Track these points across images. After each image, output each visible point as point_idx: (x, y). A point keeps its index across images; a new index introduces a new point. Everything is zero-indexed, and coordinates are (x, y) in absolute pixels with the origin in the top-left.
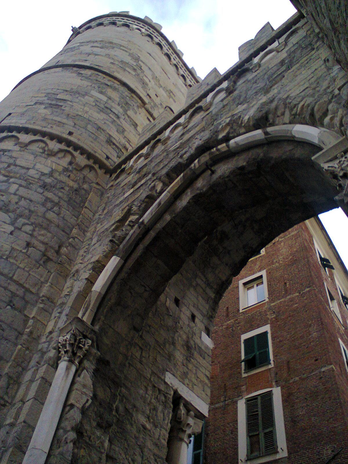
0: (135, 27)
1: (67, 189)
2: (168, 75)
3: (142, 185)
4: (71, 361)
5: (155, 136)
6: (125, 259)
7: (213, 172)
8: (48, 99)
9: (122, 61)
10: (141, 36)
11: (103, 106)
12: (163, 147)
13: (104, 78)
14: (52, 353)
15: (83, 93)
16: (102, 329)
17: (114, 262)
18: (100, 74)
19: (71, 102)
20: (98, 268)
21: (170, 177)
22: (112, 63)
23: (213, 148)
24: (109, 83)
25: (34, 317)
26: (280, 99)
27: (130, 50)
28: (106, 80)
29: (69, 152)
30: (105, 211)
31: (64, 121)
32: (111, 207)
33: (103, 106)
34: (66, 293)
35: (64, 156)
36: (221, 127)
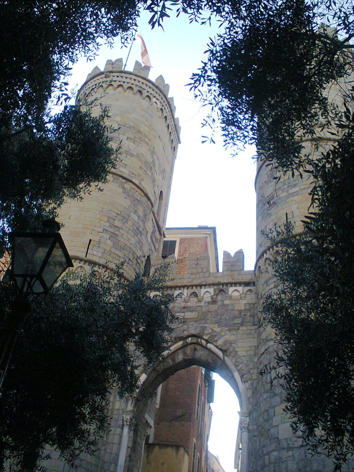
0: (154, 100)
4: (129, 429)
6: (148, 376)
7: (195, 349)
9: (146, 161)
11: (135, 229)
14: (121, 422)
15: (127, 217)
16: (137, 411)
18: (135, 187)
23: (200, 338)
24: (139, 197)
25: (112, 402)
26: (234, 349)
27: (150, 140)
28: (138, 195)
33: (135, 229)
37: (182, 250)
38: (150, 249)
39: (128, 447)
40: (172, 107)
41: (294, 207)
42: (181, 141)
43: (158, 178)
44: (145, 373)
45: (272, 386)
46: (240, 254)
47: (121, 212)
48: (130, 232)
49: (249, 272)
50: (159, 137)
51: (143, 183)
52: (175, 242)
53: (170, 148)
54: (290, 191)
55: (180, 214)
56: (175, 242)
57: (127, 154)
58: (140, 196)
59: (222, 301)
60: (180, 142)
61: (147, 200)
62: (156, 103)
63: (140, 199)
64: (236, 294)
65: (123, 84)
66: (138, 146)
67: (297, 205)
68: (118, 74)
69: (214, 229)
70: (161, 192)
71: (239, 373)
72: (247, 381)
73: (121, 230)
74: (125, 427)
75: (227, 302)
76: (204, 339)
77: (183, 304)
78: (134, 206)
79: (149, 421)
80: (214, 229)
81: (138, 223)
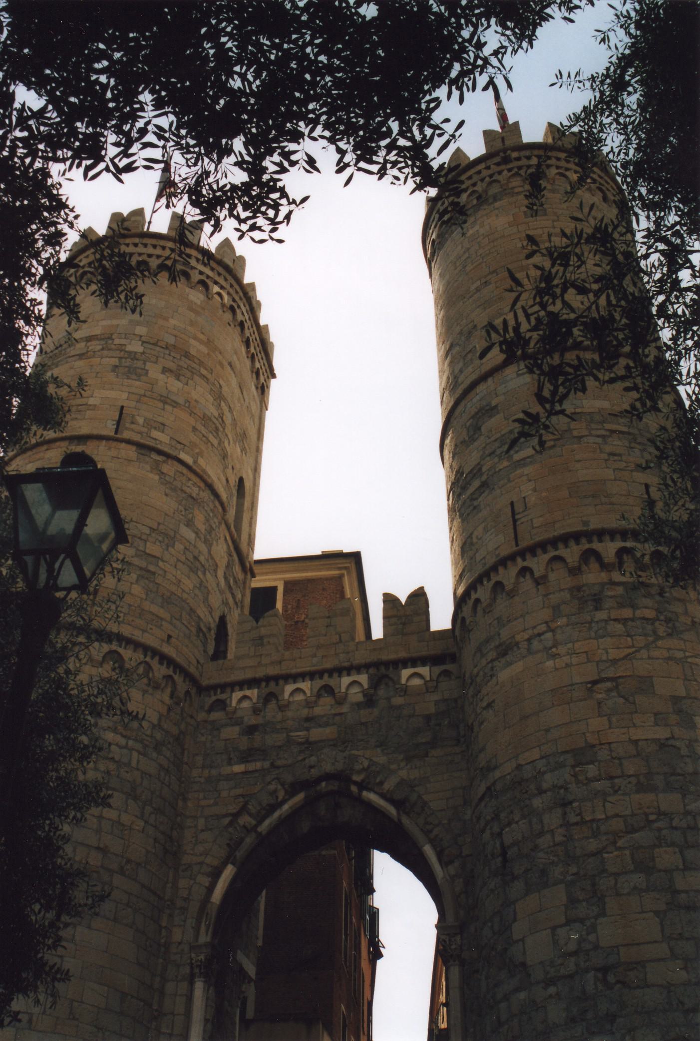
0: (216, 289)
1: (171, 740)
2: (244, 392)
3: (256, 771)
4: (205, 982)
5: (268, 679)
8: (137, 556)
9: (204, 414)
10: (221, 311)
11: (191, 558)
12: (279, 716)
13: (189, 479)
14: (187, 970)
15: (172, 534)
17: (229, 871)
18: (185, 471)
19: (163, 561)
20: (216, 874)
21: (294, 788)
22: (194, 429)
24: (194, 491)
29: (170, 677)
30: (206, 772)
31: (162, 613)
32: (214, 772)
34: (185, 896)
35: (166, 686)
36: (358, 767)
37: (289, 607)
38: (225, 603)
39: (206, 1021)
40: (254, 303)
41: (527, 489)
42: (277, 371)
43: (234, 449)
44: (233, 864)
45: (505, 860)
46: (419, 597)
47: (159, 524)
48: (180, 565)
49: (442, 634)
50: (230, 364)
51: (201, 461)
52: (274, 589)
53: (253, 388)
54: (517, 457)
55: (286, 525)
56: (274, 589)
57: (165, 403)
58: (196, 490)
59: (388, 699)
60: (274, 376)
61: (212, 498)
62: (219, 294)
63: (198, 494)
64: (416, 682)
65: (148, 260)
66: (187, 384)
67: (531, 485)
68: (137, 240)
69: (356, 558)
70: (241, 480)
71: (434, 847)
72: (451, 862)
73: (161, 564)
74: (196, 979)
75: (398, 701)
76: (355, 783)
77: (305, 712)
78: (186, 510)
79: (244, 966)
80: (356, 558)
81: (195, 547)
